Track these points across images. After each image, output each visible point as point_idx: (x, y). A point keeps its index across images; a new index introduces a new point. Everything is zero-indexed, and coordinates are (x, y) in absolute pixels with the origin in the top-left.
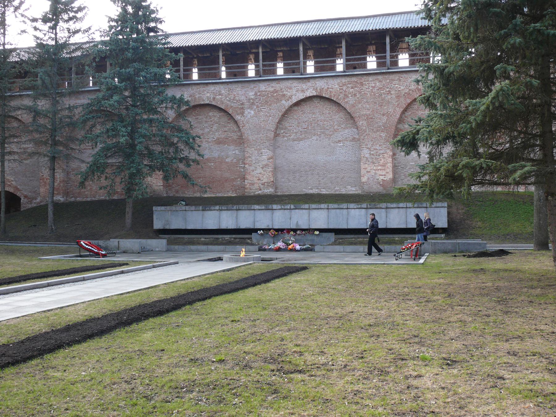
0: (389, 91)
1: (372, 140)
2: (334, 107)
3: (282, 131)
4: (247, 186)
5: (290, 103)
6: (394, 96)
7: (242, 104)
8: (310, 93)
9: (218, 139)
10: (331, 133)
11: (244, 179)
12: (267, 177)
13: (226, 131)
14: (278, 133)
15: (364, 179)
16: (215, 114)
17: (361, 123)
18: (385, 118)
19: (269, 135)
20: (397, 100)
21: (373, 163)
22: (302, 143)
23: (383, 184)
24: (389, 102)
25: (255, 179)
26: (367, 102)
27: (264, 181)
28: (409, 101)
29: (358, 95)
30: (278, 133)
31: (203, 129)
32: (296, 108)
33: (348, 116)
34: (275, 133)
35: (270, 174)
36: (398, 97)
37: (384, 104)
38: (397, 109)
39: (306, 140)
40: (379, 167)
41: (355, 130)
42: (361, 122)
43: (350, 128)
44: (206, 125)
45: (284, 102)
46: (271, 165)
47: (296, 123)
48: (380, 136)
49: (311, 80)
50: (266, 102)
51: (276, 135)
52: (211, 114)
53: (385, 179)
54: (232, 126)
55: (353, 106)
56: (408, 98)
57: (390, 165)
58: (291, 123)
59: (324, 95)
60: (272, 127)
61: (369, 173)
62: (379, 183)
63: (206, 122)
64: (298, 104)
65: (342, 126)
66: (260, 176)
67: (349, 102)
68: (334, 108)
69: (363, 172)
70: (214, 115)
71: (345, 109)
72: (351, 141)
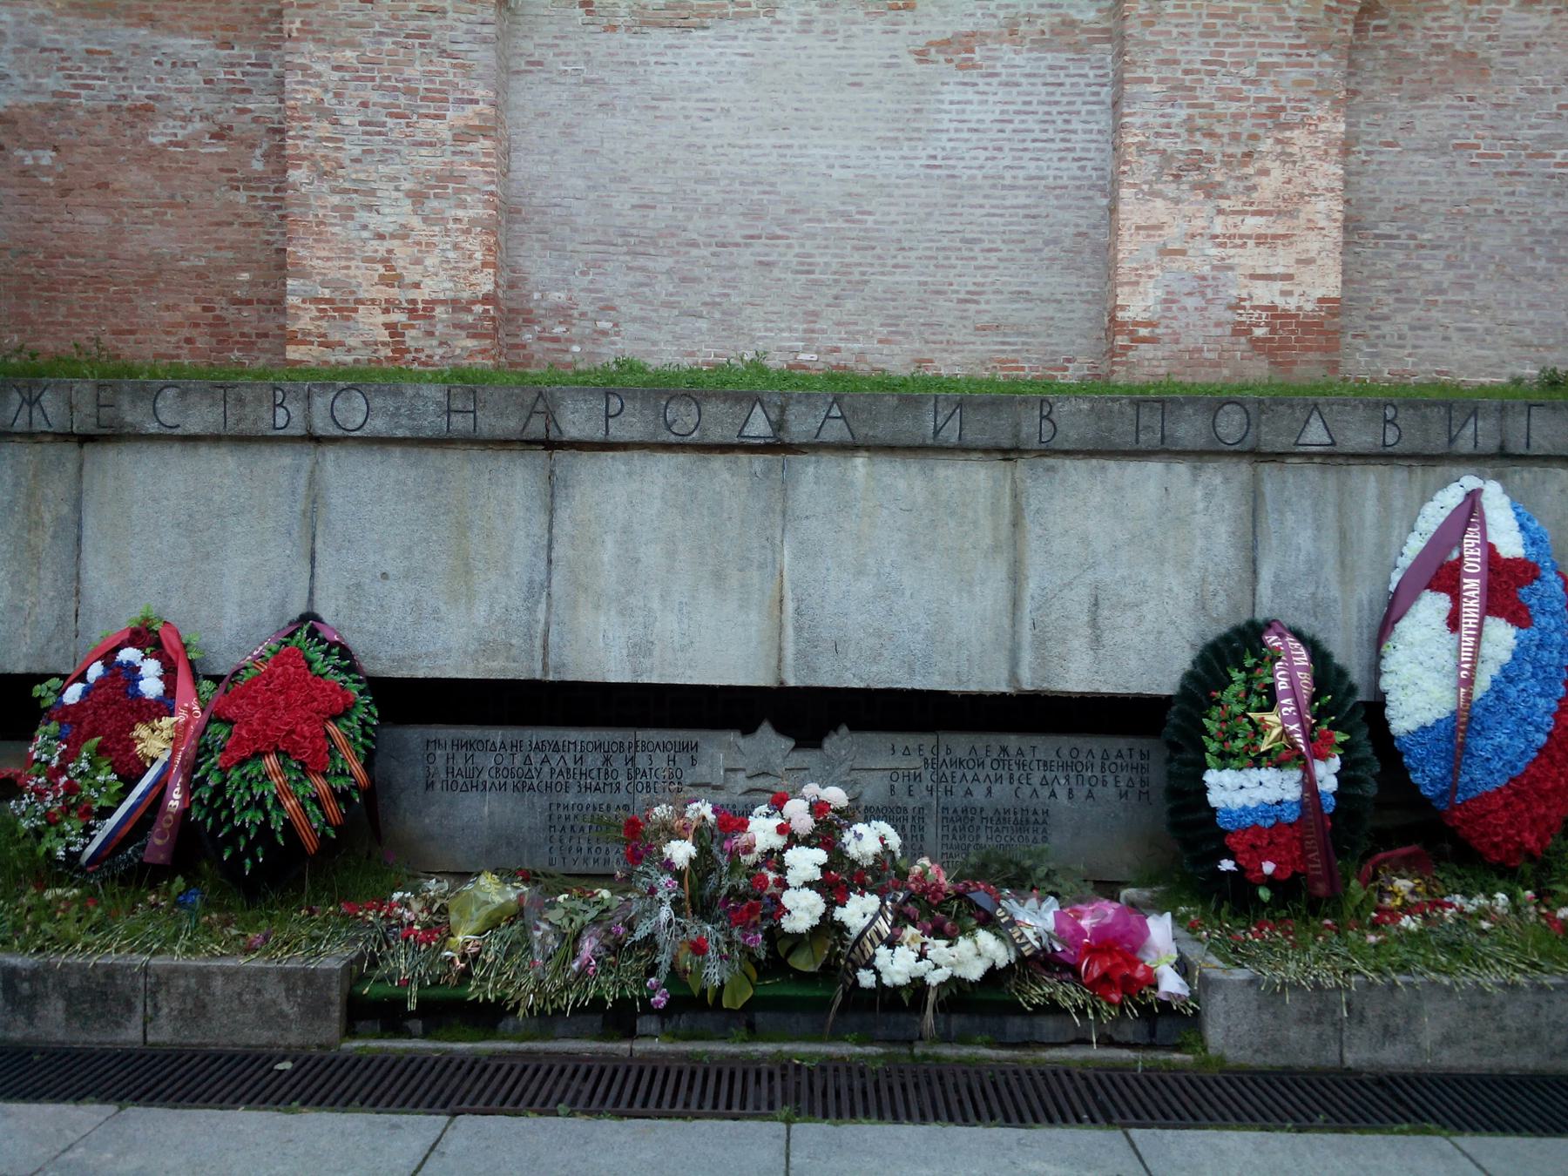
11: (280, 266)
15: (1137, 304)
21: (1210, 190)
22: (698, 44)
23: (1286, 333)
35: (476, 246)
39: (729, 28)
40: (1252, 224)
46: (479, 178)
53: (1292, 304)
57: (1326, 209)
61: (1179, 263)
62: (1240, 330)
66: (402, 253)
69: (1131, 250)
72: (1042, 43)
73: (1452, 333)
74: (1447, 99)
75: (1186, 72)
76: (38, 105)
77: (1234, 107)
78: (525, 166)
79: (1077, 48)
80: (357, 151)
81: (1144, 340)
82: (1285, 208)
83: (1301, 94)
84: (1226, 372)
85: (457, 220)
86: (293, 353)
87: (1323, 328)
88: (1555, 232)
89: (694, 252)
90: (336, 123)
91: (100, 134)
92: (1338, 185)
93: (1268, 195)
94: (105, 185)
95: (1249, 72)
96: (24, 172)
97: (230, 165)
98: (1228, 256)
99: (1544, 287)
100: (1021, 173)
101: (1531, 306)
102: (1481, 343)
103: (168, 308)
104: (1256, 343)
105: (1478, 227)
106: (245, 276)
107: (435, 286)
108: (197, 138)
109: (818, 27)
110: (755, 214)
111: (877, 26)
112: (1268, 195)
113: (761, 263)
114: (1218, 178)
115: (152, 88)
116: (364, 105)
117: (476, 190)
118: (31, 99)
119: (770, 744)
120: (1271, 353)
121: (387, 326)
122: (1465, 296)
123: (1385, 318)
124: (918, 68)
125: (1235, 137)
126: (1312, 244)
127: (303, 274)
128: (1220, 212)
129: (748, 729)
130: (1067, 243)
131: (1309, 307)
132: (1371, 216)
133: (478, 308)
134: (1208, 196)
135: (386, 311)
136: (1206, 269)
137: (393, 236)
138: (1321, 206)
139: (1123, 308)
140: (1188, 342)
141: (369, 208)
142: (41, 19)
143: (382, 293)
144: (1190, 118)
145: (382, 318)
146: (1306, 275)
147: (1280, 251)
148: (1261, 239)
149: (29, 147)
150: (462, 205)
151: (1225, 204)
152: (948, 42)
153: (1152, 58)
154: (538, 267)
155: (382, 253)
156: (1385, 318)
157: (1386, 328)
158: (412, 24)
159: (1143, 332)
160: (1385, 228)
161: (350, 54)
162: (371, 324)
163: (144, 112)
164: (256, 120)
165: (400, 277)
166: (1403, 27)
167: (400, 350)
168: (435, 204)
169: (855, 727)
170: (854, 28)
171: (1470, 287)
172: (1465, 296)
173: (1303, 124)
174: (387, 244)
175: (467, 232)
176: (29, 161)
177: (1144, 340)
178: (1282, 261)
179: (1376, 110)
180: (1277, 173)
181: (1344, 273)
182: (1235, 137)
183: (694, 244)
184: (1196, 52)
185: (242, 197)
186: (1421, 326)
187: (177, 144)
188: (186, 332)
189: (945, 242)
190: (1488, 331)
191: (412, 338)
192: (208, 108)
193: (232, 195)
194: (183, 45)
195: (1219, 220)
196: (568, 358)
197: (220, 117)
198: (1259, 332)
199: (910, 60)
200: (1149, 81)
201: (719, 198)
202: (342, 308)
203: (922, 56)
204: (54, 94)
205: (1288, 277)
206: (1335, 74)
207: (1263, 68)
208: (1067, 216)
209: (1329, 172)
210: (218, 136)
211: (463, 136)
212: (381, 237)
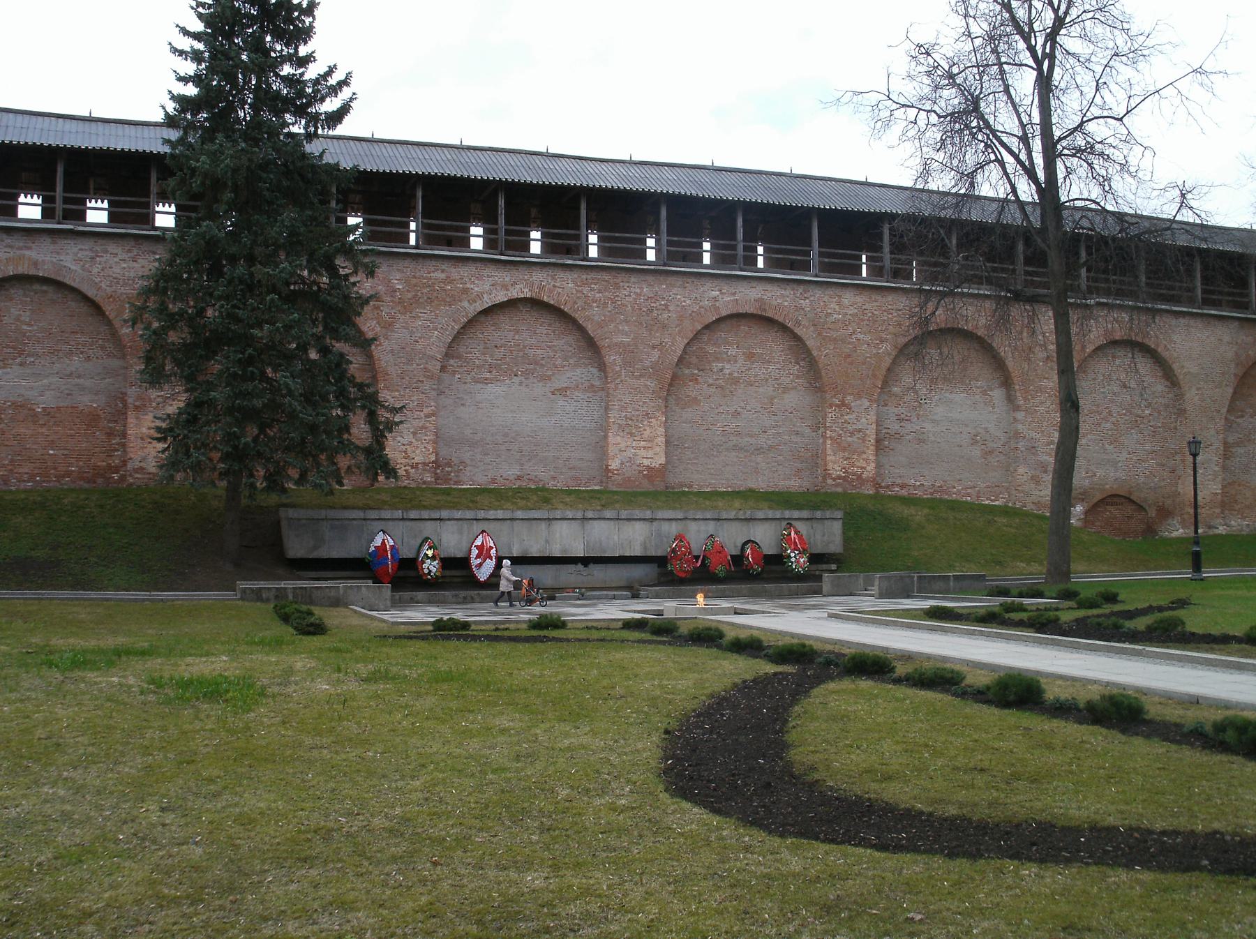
0: (666, 305)
5: (479, 307)
8: (520, 291)
10: (550, 373)
15: (614, 464)
17: (611, 358)
18: (656, 353)
21: (632, 434)
23: (652, 474)
24: (664, 327)
26: (626, 321)
29: (610, 307)
32: (482, 319)
36: (681, 318)
40: (643, 443)
41: (595, 371)
43: (586, 365)
45: (466, 304)
49: (521, 268)
50: (430, 301)
51: (443, 368)
57: (661, 440)
58: (472, 348)
59: (546, 299)
60: (437, 351)
62: (640, 472)
64: (487, 312)
65: (571, 361)
67: (591, 317)
68: (558, 326)
69: (612, 450)
71: (581, 329)
72: (585, 390)
79: (595, 392)
82: (650, 440)
87: (662, 471)
98: (638, 450)
110: (506, 435)
119: (580, 567)
126: (658, 449)
143: (404, 461)
180: (648, 431)
186: (685, 469)
203: (553, 393)
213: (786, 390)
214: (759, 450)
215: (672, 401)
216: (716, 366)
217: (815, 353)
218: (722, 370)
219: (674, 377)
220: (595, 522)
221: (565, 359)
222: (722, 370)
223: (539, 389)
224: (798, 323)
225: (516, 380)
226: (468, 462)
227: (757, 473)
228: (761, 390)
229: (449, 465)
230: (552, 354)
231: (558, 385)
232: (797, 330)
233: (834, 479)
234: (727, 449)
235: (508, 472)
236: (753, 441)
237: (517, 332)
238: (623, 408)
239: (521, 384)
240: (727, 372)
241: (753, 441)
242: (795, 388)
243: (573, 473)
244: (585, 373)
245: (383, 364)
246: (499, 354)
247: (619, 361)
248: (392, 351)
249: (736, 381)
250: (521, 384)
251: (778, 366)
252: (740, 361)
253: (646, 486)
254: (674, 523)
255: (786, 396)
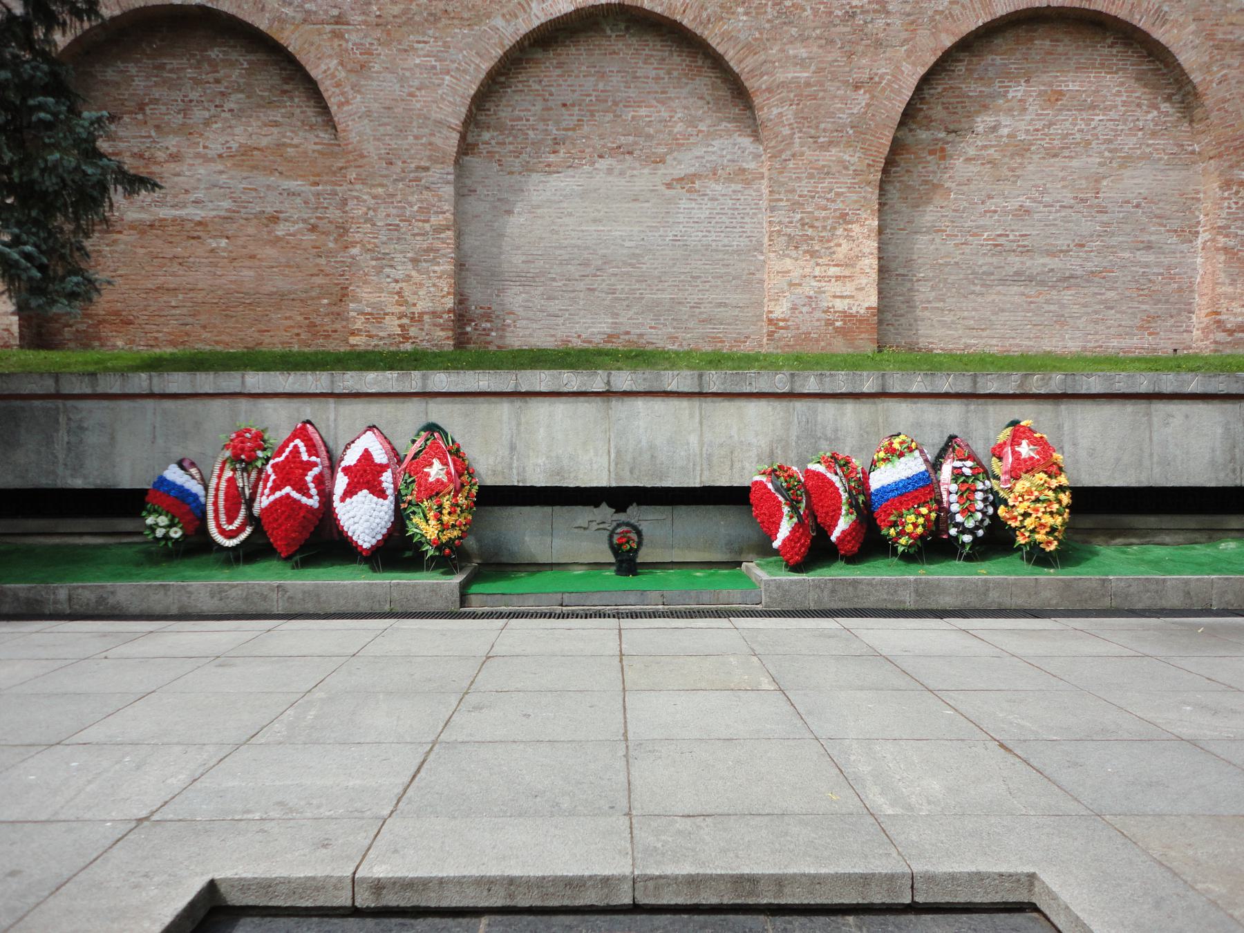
1: (811, 176)
2: (676, 59)
3: (486, 136)
4: (358, 325)
6: (897, 22)
7: (339, 20)
9: (246, 151)
10: (662, 150)
11: (343, 295)
12: (431, 293)
13: (276, 124)
14: (470, 140)
15: (780, 310)
16: (234, 56)
18: (862, 98)
19: (438, 141)
20: (904, 35)
21: (813, 254)
24: (878, 44)
25: (384, 297)
26: (803, 39)
27: (419, 308)
28: (948, 41)
30: (470, 140)
31: (185, 112)
33: (724, 92)
34: (463, 137)
35: (445, 285)
36: (912, 25)
37: (861, 48)
38: (906, 67)
39: (571, 172)
40: (833, 271)
41: (746, 142)
42: (775, 111)
43: (729, 133)
44: (194, 95)
45: (499, 22)
47: (539, 107)
48: (841, 161)
50: (434, 19)
51: (466, 148)
52: (214, 53)
54: (299, 106)
55: (750, 48)
56: (947, 31)
57: (870, 264)
60: (453, 110)
61: (799, 290)
62: (829, 323)
63: (197, 82)
65: (703, 127)
68: (678, 60)
70: (234, 66)
71: (716, 62)
72: (729, 180)
73: (935, 323)
74: (931, 208)
75: (800, 196)
76: (219, 217)
77: (824, 213)
78: (470, 242)
80: (385, 239)
81: (782, 328)
82: (850, 263)
83: (856, 207)
84: (823, 344)
85: (435, 272)
86: (353, 340)
88: (984, 273)
89: (555, 284)
90: (374, 225)
91: (251, 231)
92: (876, 252)
93: (841, 256)
94: (253, 257)
95: (831, 195)
96: (212, 251)
97: (318, 244)
99: (979, 299)
100: (720, 244)
101: (974, 309)
102: (950, 328)
103: (286, 318)
104: (836, 329)
105: (947, 270)
106: (326, 301)
107: (422, 306)
108: (299, 231)
109: (616, 172)
110: (586, 264)
111: (646, 171)
112: (841, 256)
113: (589, 289)
114: (817, 248)
115: (277, 207)
116: (388, 215)
117: (444, 255)
118: (214, 213)
120: (844, 335)
121: (400, 326)
122: (941, 305)
123: (902, 315)
124: (667, 192)
125: (824, 228)
126: (864, 281)
127: (356, 300)
128: (818, 264)
129: (597, 505)
130: (744, 278)
131: (862, 311)
132: (893, 265)
133: (446, 316)
134: (812, 257)
135: (399, 318)
136: (812, 293)
137: (403, 281)
138: (867, 262)
139: (771, 312)
140: (803, 329)
141: (391, 266)
142: (221, 172)
144: (802, 219)
145: (398, 322)
146: (860, 296)
147: (848, 284)
148: (838, 278)
149: (215, 237)
150: (438, 264)
151: (820, 261)
152: (682, 179)
153: (782, 190)
154: (477, 296)
155: (397, 289)
156: (902, 315)
157: (903, 320)
158: (412, 175)
159: (781, 324)
160: (901, 271)
161: (380, 190)
162: (392, 326)
163: (274, 219)
164: (330, 222)
165: (406, 301)
166: (908, 171)
167: (406, 338)
168: (424, 264)
169: (639, 504)
170: (635, 172)
171: (944, 301)
172: (941, 305)
173: (857, 221)
174: (399, 285)
175: (440, 277)
176: (214, 245)
177: (782, 328)
178: (849, 289)
179: (895, 213)
181: (880, 293)
182: (824, 228)
183: (554, 280)
184: (805, 187)
185: (323, 261)
187: (290, 235)
188: (296, 331)
189: (683, 277)
190: (953, 322)
191: (413, 332)
192: (306, 216)
193: (318, 260)
194: (293, 185)
195: (817, 269)
196: (489, 339)
197: (312, 221)
198: (838, 324)
199: (663, 188)
200: (781, 200)
201: (567, 257)
202: (377, 317)
203: (669, 186)
204: (228, 210)
205: (852, 297)
206: (875, 196)
207: (838, 194)
208: (744, 265)
209: (872, 245)
210: (314, 228)
211: (438, 230)
212: (397, 281)
213: (1127, 161)
214: (1068, 280)
215: (894, 193)
216: (982, 122)
217: (1196, 77)
218: (994, 129)
219: (897, 147)
220: (640, 404)
221: (692, 122)
222: (994, 129)
223: (644, 178)
224: (1161, 17)
225: (602, 164)
226: (521, 312)
227: (1063, 324)
228: (1075, 163)
229: (487, 317)
230: (665, 114)
231: (680, 171)
232: (1158, 34)
233: (1231, 332)
234: (1003, 281)
235: (590, 328)
236: (1054, 263)
237: (602, 75)
238: (795, 206)
239: (610, 171)
240: (1005, 131)
241: (1054, 263)
242: (1146, 157)
243: (708, 329)
244: (733, 146)
245: (354, 137)
246: (569, 119)
247: (789, 113)
248: (368, 114)
249: (1022, 150)
250: (610, 171)
251: (1113, 114)
252: (1033, 108)
253: (840, 346)
254: (849, 407)
255: (1127, 173)
